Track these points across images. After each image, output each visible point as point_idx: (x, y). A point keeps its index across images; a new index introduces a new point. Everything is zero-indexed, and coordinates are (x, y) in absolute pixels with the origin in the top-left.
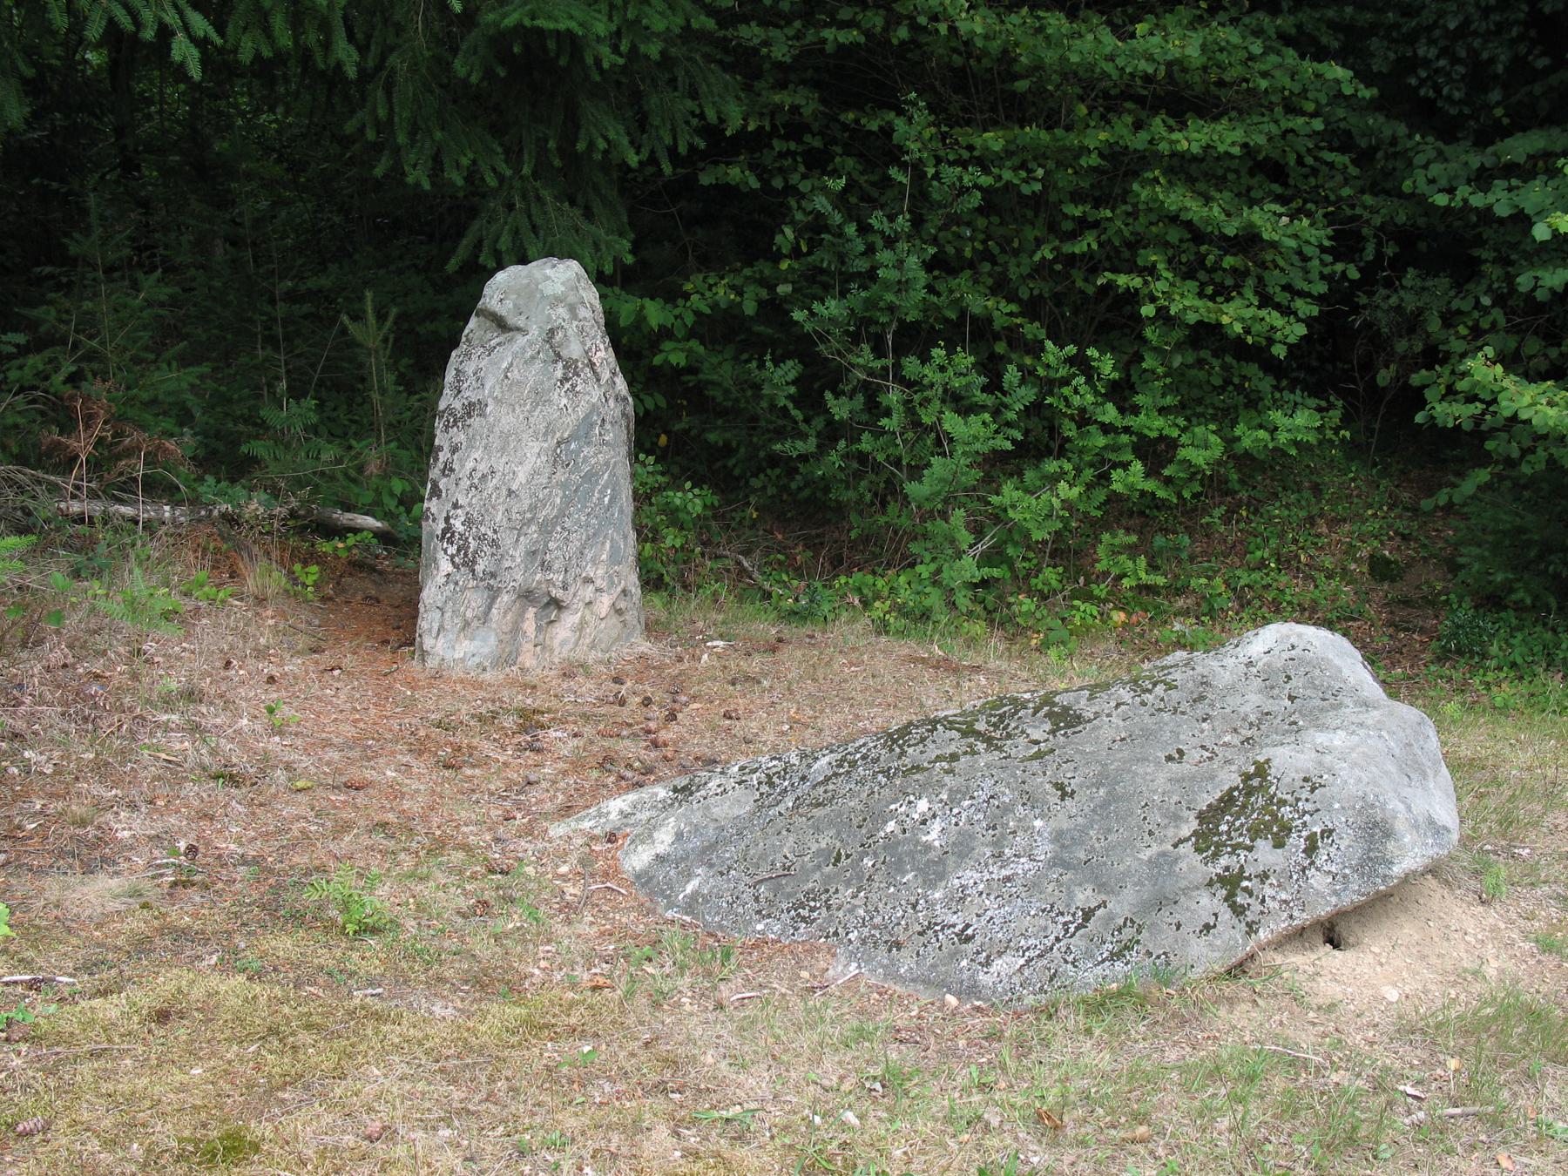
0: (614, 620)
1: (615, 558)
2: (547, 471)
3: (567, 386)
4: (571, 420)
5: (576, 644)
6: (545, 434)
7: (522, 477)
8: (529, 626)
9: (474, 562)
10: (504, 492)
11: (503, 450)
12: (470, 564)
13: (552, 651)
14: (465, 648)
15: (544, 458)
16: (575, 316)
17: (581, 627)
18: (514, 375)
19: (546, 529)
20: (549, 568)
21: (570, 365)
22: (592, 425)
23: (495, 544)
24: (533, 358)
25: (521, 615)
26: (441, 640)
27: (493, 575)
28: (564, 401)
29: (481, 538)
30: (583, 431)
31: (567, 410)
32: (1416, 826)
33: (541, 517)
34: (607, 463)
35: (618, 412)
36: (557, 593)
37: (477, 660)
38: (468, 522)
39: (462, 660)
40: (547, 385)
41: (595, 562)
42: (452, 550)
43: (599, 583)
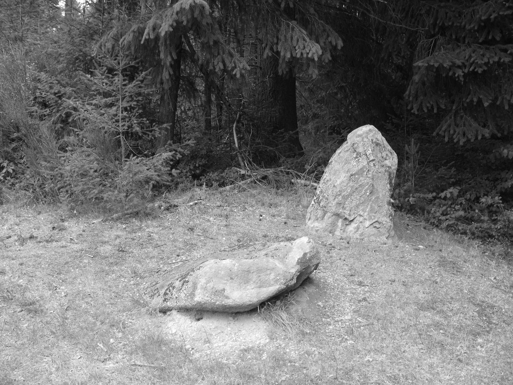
0: (374, 229)
1: (372, 210)
2: (347, 182)
3: (357, 159)
4: (355, 170)
5: (355, 232)
6: (347, 172)
7: (338, 182)
8: (340, 223)
9: (320, 202)
10: (333, 186)
11: (334, 174)
12: (319, 203)
13: (347, 232)
14: (316, 224)
15: (346, 178)
16: (363, 140)
17: (358, 228)
18: (341, 155)
19: (345, 198)
20: (345, 209)
21: (359, 154)
22: (364, 171)
23: (327, 199)
24: (347, 151)
25: (338, 221)
26: (310, 221)
27: (325, 207)
28: (355, 164)
29: (324, 197)
30: (360, 172)
31: (355, 166)
32: (205, 289)
33: (343, 194)
34: (368, 183)
35: (383, 170)
36: (348, 217)
37: (318, 229)
38: (321, 192)
39: (313, 228)
40: (350, 158)
41: (363, 210)
42: (315, 198)
43: (365, 217)
